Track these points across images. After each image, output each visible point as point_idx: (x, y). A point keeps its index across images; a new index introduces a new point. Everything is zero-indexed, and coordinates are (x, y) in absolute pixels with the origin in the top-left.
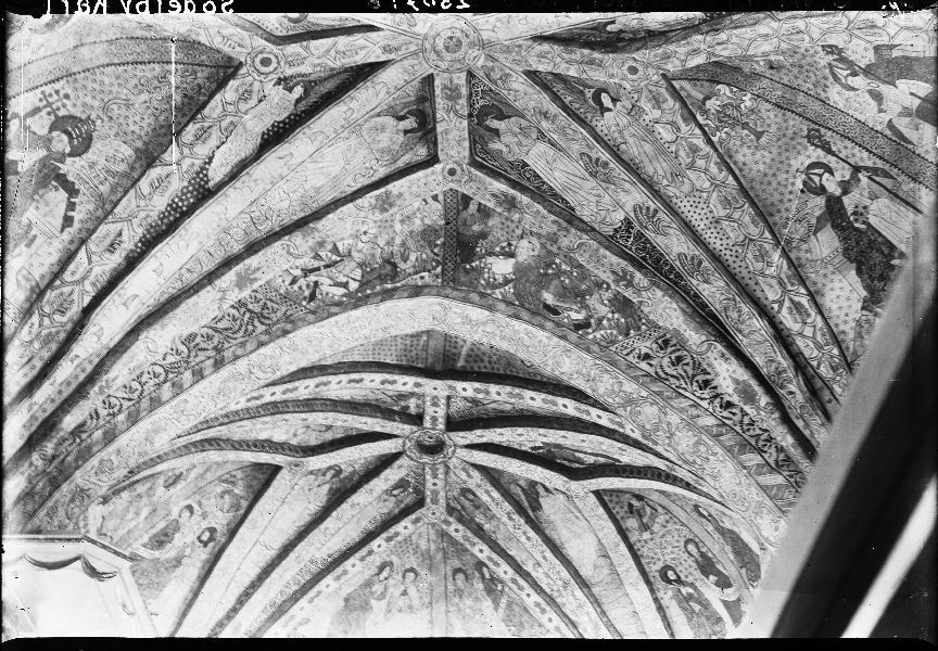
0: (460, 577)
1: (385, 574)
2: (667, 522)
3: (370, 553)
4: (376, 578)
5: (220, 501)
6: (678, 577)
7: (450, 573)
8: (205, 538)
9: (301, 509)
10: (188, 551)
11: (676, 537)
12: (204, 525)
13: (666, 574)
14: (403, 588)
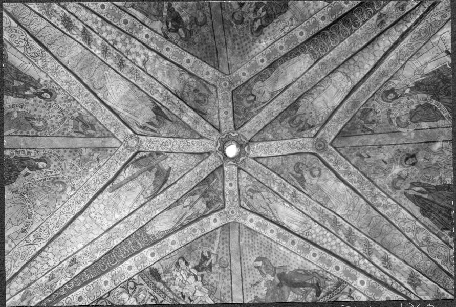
0: (200, 20)
1: (257, 25)
2: (64, 130)
3: (269, 56)
4: (264, 22)
5: (376, 118)
6: (41, 97)
7: (208, 19)
8: (392, 95)
9: (318, 99)
10: (408, 91)
11: (55, 124)
13: (51, 94)
14: (243, 9)
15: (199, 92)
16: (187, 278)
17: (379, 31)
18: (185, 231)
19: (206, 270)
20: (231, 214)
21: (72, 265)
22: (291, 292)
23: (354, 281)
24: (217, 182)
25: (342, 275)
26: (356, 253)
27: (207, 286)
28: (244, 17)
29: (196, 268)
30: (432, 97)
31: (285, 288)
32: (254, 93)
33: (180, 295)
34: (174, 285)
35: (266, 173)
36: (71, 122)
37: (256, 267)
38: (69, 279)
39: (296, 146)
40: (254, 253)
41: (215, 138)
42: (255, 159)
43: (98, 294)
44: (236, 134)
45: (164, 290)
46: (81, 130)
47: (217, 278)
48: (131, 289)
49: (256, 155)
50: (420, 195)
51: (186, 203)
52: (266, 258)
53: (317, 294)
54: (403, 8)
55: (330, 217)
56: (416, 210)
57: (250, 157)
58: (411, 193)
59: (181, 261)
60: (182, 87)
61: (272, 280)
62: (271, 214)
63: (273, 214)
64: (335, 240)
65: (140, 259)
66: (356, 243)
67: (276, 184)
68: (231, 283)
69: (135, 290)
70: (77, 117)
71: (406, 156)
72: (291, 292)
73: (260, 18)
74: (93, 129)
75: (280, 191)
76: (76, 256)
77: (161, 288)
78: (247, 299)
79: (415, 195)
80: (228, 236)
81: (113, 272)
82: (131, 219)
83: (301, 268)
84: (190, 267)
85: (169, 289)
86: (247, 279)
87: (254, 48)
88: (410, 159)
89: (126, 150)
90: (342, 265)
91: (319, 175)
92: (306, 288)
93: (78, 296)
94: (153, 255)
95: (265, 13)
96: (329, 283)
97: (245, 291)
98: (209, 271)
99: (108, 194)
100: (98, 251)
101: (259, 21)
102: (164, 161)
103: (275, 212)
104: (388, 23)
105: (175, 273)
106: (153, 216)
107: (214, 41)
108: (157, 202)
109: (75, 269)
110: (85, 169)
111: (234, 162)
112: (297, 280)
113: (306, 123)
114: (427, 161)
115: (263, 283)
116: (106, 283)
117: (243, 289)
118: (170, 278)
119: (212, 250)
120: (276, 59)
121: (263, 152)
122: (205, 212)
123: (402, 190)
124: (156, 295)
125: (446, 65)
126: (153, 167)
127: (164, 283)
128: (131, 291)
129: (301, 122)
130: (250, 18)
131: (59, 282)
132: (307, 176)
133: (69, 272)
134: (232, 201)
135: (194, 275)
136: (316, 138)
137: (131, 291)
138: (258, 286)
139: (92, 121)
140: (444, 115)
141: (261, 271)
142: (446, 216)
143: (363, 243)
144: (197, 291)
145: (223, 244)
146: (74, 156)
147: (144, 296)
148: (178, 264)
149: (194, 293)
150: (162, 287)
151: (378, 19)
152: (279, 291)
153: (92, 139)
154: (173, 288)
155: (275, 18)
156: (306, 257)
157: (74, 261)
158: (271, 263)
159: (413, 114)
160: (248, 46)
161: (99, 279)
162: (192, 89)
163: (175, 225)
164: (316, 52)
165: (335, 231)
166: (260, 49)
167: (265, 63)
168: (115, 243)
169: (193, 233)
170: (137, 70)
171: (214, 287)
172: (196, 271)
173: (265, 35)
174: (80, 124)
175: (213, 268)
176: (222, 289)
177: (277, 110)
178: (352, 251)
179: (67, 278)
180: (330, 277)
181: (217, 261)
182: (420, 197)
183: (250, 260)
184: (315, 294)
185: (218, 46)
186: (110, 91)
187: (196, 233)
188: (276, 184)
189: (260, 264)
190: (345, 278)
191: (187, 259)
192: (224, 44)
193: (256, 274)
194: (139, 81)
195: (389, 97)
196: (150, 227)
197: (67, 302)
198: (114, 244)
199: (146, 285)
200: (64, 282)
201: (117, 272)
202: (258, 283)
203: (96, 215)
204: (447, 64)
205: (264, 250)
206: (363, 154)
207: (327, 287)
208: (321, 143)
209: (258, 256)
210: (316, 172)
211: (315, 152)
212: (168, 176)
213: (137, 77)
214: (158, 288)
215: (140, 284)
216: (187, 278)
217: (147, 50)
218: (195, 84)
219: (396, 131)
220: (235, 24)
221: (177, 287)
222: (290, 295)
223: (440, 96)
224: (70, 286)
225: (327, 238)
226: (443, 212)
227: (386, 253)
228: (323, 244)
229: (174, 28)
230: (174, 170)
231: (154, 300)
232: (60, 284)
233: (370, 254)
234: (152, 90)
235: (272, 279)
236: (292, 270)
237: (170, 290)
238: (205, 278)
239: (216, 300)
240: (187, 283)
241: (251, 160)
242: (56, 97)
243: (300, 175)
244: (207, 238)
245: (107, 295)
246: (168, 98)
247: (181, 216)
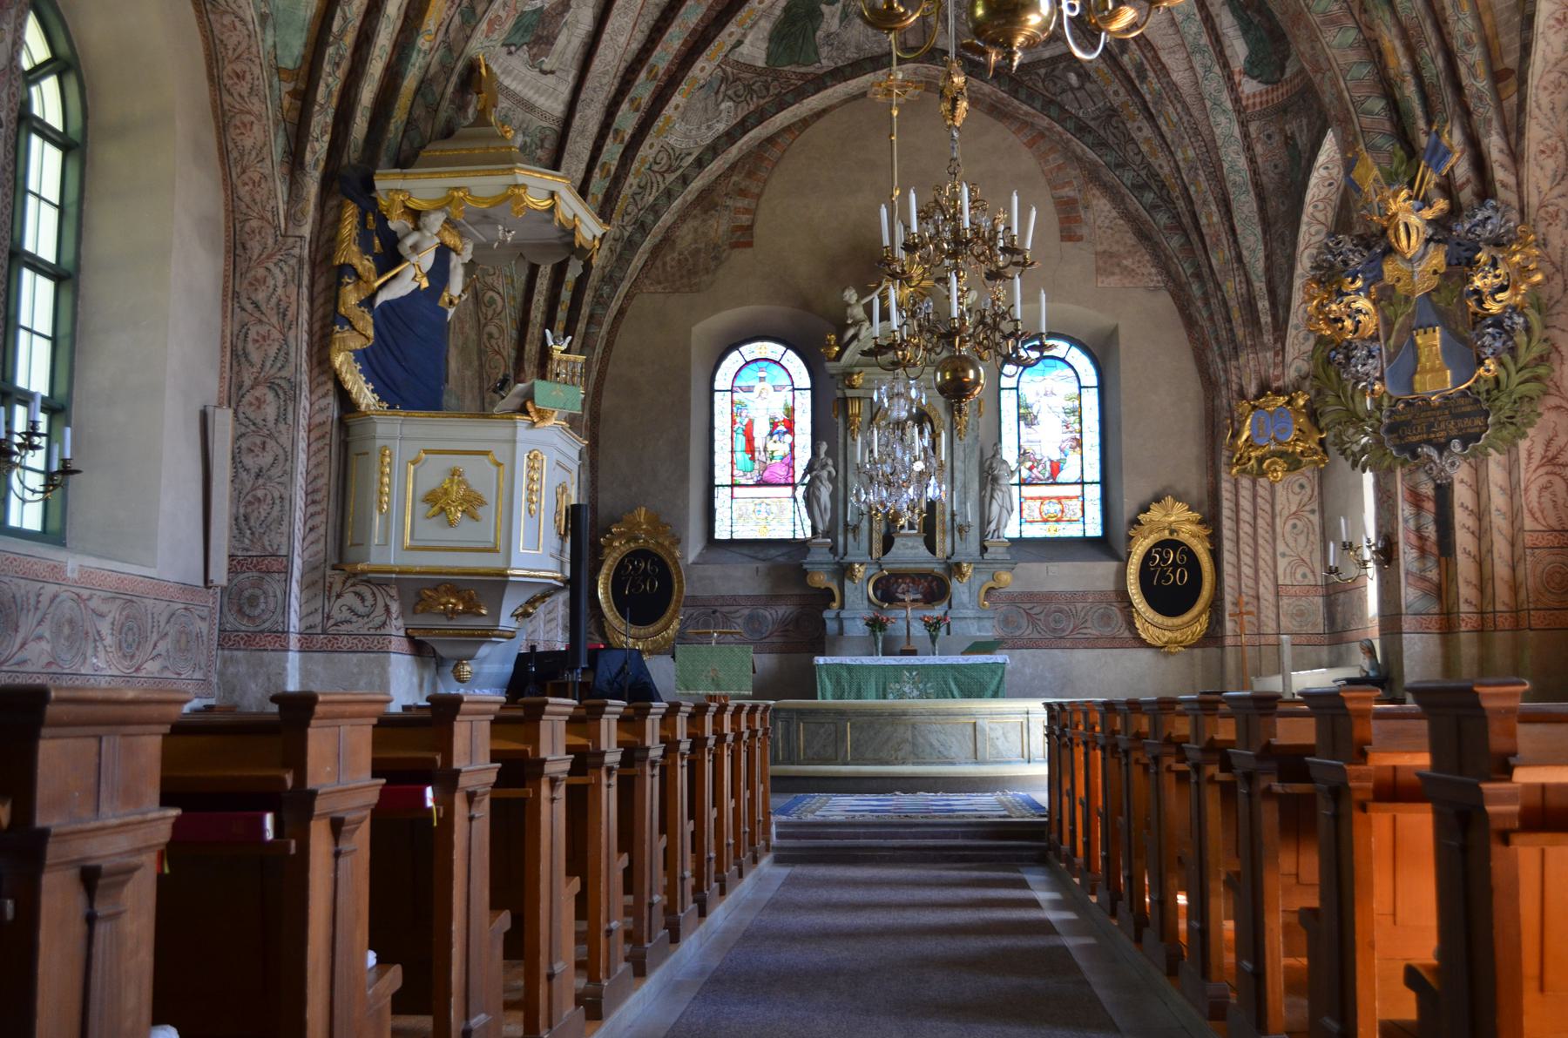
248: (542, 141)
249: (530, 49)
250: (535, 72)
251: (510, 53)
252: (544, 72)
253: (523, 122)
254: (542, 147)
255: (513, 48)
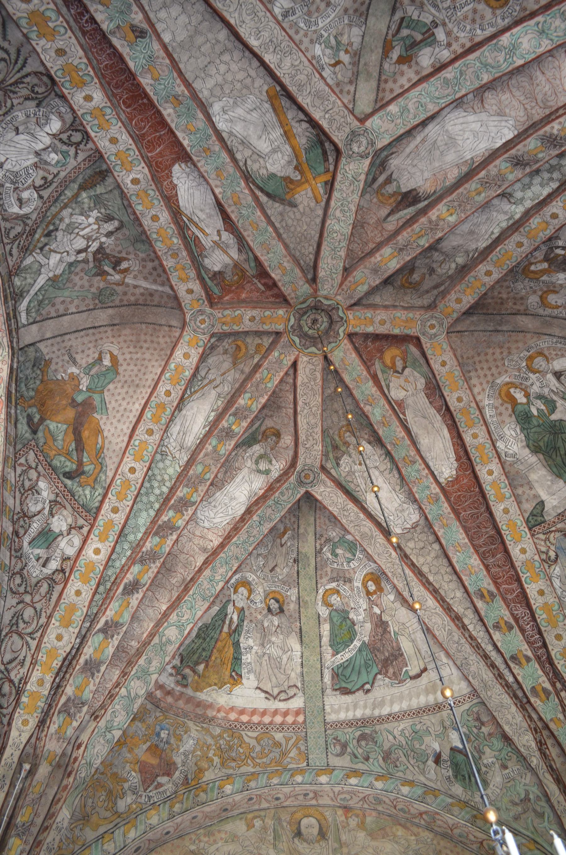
1: (520, 397)
4: (519, 408)
8: (372, 587)
10: (377, 610)
12: (358, 584)
14: (550, 376)
15: (427, 276)
16: (83, 237)
17: (471, 589)
18: (175, 240)
19: (95, 267)
20: (201, 318)
21: (133, 31)
22: (65, 427)
23: (97, 539)
24: (258, 290)
25: (105, 518)
26: (140, 535)
27: (67, 272)
28: (537, 375)
29: (101, 249)
30: (364, 642)
31: (70, 414)
32: (407, 371)
33: (51, 228)
34: (72, 215)
35: (269, 385)
36: (427, 19)
37: (101, 353)
38: (104, 27)
39: (311, 438)
40: (126, 350)
41: (339, 298)
42: (294, 365)
43: (67, 85)
44: (342, 334)
45: (62, 198)
46: (405, 32)
47: (82, 287)
48: (69, 137)
49: (300, 366)
50: (227, 622)
51: (226, 236)
52: (117, 373)
53: (69, 473)
54: (497, 626)
55: (195, 495)
56: (207, 619)
57: (298, 355)
58: (230, 609)
59: (116, 223)
60: (444, 250)
61: (81, 387)
62: (197, 388)
63: (196, 392)
64: (157, 500)
65: (130, 159)
66: (157, 539)
67: (250, 403)
68: (72, 313)
69: (65, 144)
70: (433, 34)
71: (281, 600)
72: (65, 427)
73: (528, 403)
74: (402, 60)
75: (237, 409)
76: (150, 36)
77: (66, 192)
78: (47, 346)
79: (226, 615)
80: (155, 303)
81: (108, 111)
82: (211, 142)
83: (106, 442)
84: (103, 239)
85: (66, 206)
86: (79, 340)
87: (481, 384)
88: (277, 605)
89: (347, 130)
90: (119, 518)
91: (259, 471)
92: (75, 453)
93: (67, 50)
94: (135, 181)
95: (535, 413)
96: (87, 492)
97: (59, 339)
98: (93, 273)
99: (266, 88)
100: (156, 80)
101: (524, 400)
102: (310, 194)
103: (198, 395)
104: (480, 604)
105: (95, 213)
106: (210, 181)
107: (509, 312)
108: (238, 189)
109: (125, 38)
110: (322, 36)
111: (292, 327)
112: (86, 434)
113: (344, 453)
114: (274, 629)
115: (74, 370)
116: (88, 98)
117: (61, 335)
118: (86, 206)
119: (131, 276)
120: (458, 424)
121: (306, 381)
122: (207, 270)
123: (233, 597)
124: (55, 185)
125: (407, 666)
126: (302, 173)
127: (77, 195)
128: (64, 137)
129: (347, 444)
130: (532, 385)
131: (100, 7)
132: (257, 449)
133: (118, 27)
134: (224, 320)
135: (88, 247)
136: (319, 471)
137: (64, 137)
138: (68, 362)
139: (417, 63)
140: (339, 656)
141: (93, 364)
142: (199, 658)
143: (157, 549)
144: (58, 256)
145: (142, 294)
146: (351, 12)
147: (53, 162)
148: (109, 218)
149: (55, 252)
150: (69, 193)
151: (488, 591)
152: (64, 402)
153: (380, 51)
154: (65, 213)
155: (522, 429)
156: (127, 454)
157: (140, 34)
158: (109, 383)
159: (344, 614)
160: (488, 373)
161: (98, 85)
162: (434, 265)
163: (186, 216)
164: (456, 487)
165: (173, 505)
166: (479, 393)
167: (457, 404)
168: (168, 112)
169: (170, 253)
170: (500, 186)
171: (64, 285)
172: (95, 249)
173: (500, 408)
174: (419, 37)
175: (99, 278)
176: (62, 299)
177: (374, 414)
178: (143, 530)
179: (107, 23)
180: (97, 494)
181: (110, 284)
182: (224, 622)
183: (112, 343)
184: (67, 469)
185: (498, 318)
186: (471, 118)
187: (169, 258)
188: (250, 403)
189: (107, 362)
190: (101, 523)
191: (119, 235)
192: (500, 328)
193: (88, 356)
194: (479, 186)
195: (370, 583)
196: (188, 170)
197: (57, 29)
198: (165, 109)
199: (75, 164)
200: (99, 17)
201: (107, 117)
202: (75, 362)
203: (226, 63)
204: (409, 668)
205: (132, 370)
206: (286, 536)
207: (80, 489)
208: (311, 479)
209: (120, 358)
210: (263, 466)
211: (299, 467)
212: (282, 201)
213: (486, 183)
214: (66, 187)
215: (77, 153)
216: (83, 237)
217: (528, 204)
218: (444, 271)
219: (319, 586)
220: (528, 354)
221: (67, 221)
222: (59, 425)
223: (364, 653)
224: (87, 22)
225: (159, 487)
226: (204, 654)
227: (144, 585)
228: (150, 481)
229: (552, 255)
230: (291, 214)
231: (45, 183)
232: (96, 10)
233: (141, 561)
234: (456, 204)
235: (83, 387)
236: (101, 423)
237: (62, 209)
238: (82, 265)
239: (43, 292)
240: (73, 236)
241: (293, 358)
242: (489, 5)
243: (260, 437)
244: (155, 269)
245: (59, 93)
246: (431, 229)
247: (202, 225)
248: (478, 719)
249: (386, 674)
250: (409, 684)
251: (368, 691)
252: (418, 676)
253: (442, 722)
254: (483, 724)
255: (367, 687)
